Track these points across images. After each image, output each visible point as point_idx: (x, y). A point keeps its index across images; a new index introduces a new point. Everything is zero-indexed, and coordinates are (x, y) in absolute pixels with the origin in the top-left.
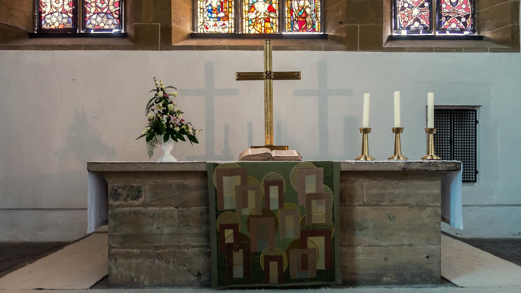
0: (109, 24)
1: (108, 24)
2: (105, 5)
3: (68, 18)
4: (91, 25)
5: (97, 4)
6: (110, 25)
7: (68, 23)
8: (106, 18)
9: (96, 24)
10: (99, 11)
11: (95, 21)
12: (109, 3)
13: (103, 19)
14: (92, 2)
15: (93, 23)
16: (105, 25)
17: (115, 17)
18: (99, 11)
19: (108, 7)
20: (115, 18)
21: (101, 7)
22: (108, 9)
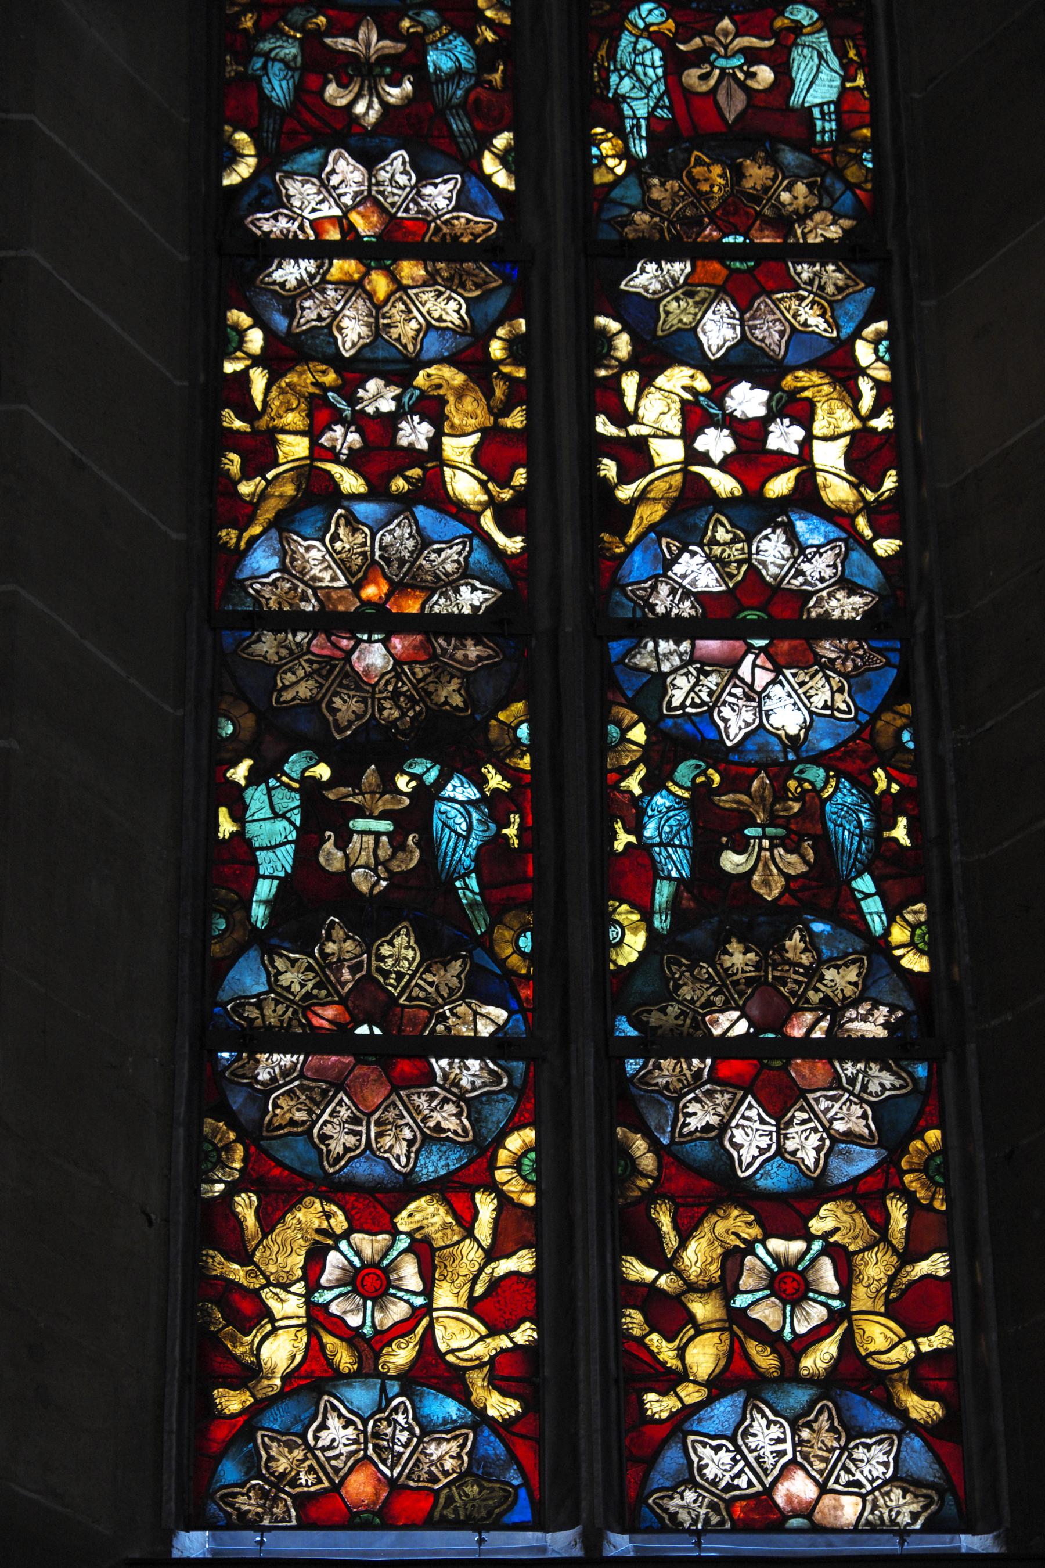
0: (858, 1476)
1: (858, 1484)
2: (817, 1314)
3: (475, 1427)
4: (690, 1496)
5: (741, 1301)
6: (869, 1487)
7: (469, 1472)
8: (832, 1429)
9: (742, 1482)
10: (765, 1360)
11: (725, 1457)
12: (845, 1294)
13: (805, 1434)
14: (691, 1288)
15: (710, 1473)
16: (823, 1489)
17: (914, 1415)
18: (765, 1360)
19: (845, 1325)
20: (911, 1426)
21: (775, 1328)
22: (848, 1344)
